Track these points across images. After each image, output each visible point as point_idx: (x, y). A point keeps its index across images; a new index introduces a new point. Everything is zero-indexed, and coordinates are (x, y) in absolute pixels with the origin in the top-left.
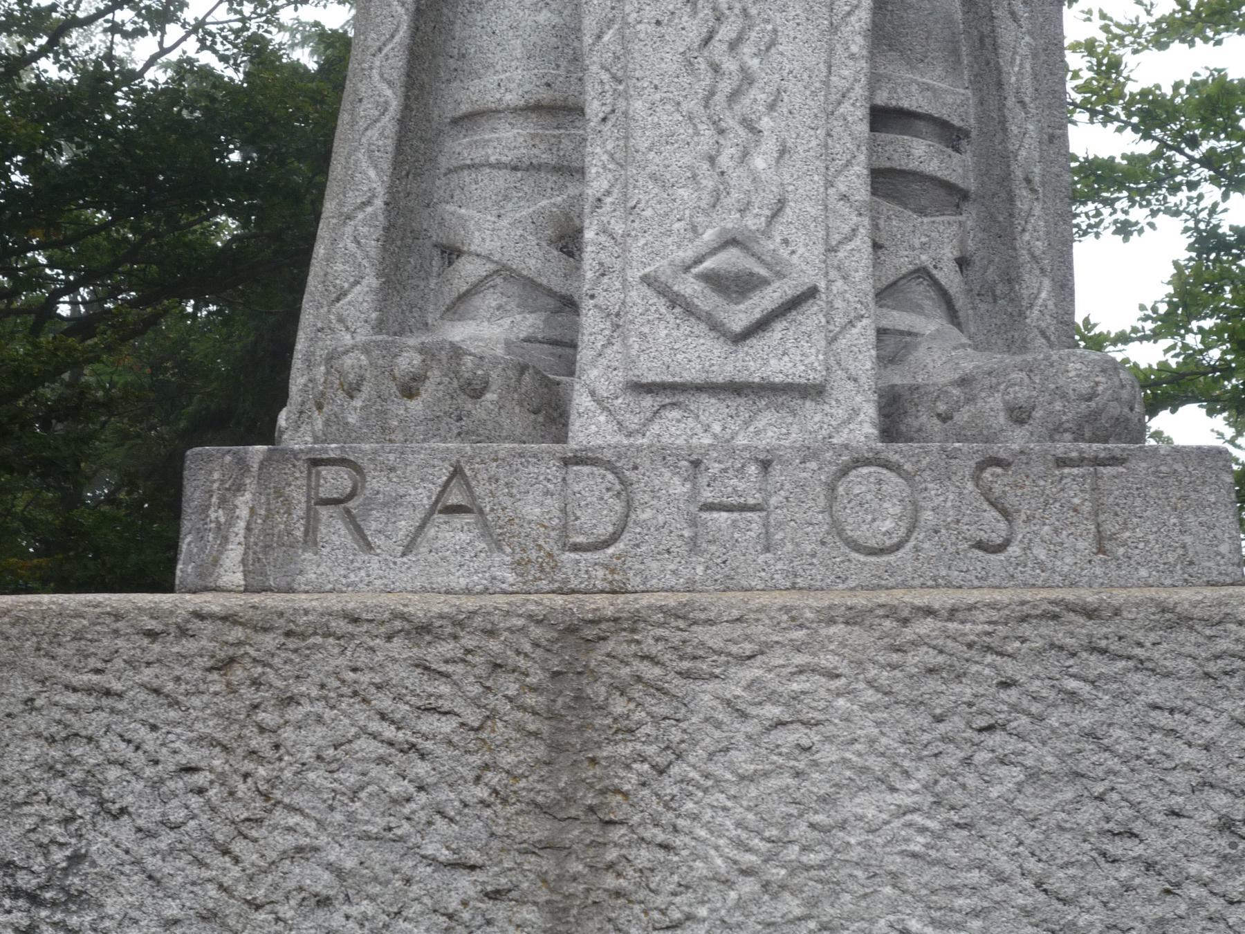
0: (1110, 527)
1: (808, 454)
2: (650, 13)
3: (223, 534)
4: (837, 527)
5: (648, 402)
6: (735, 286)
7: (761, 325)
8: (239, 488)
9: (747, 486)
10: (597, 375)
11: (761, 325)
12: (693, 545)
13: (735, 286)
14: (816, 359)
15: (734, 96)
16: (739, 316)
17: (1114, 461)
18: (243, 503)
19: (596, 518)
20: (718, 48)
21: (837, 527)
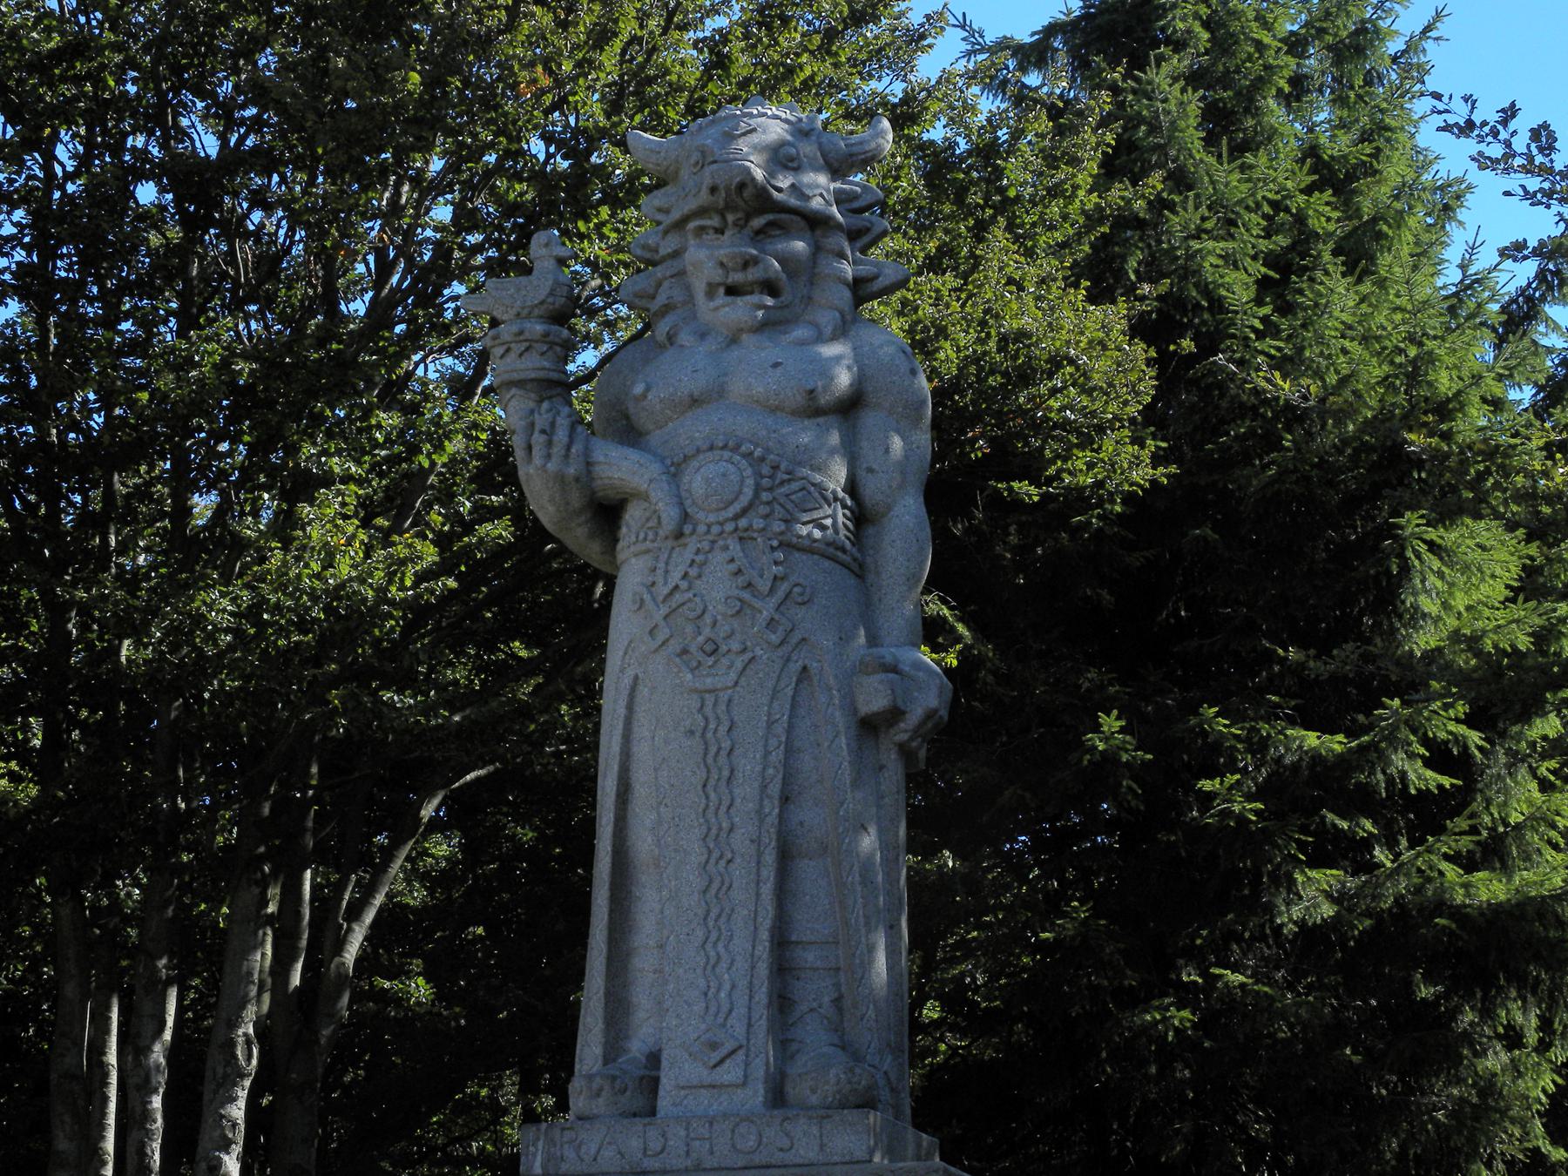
0: (825, 1140)
1: (725, 1116)
2: (685, 930)
3: (534, 1155)
4: (733, 1146)
5: (683, 1093)
6: (714, 1046)
7: (721, 1062)
8: (538, 1139)
9: (705, 1132)
10: (666, 1083)
11: (721, 1062)
12: (688, 1153)
13: (714, 1046)
14: (741, 1073)
15: (714, 967)
16: (716, 1056)
17: (828, 1117)
18: (540, 1144)
19: (655, 1145)
20: (709, 946)
21: (733, 1146)
